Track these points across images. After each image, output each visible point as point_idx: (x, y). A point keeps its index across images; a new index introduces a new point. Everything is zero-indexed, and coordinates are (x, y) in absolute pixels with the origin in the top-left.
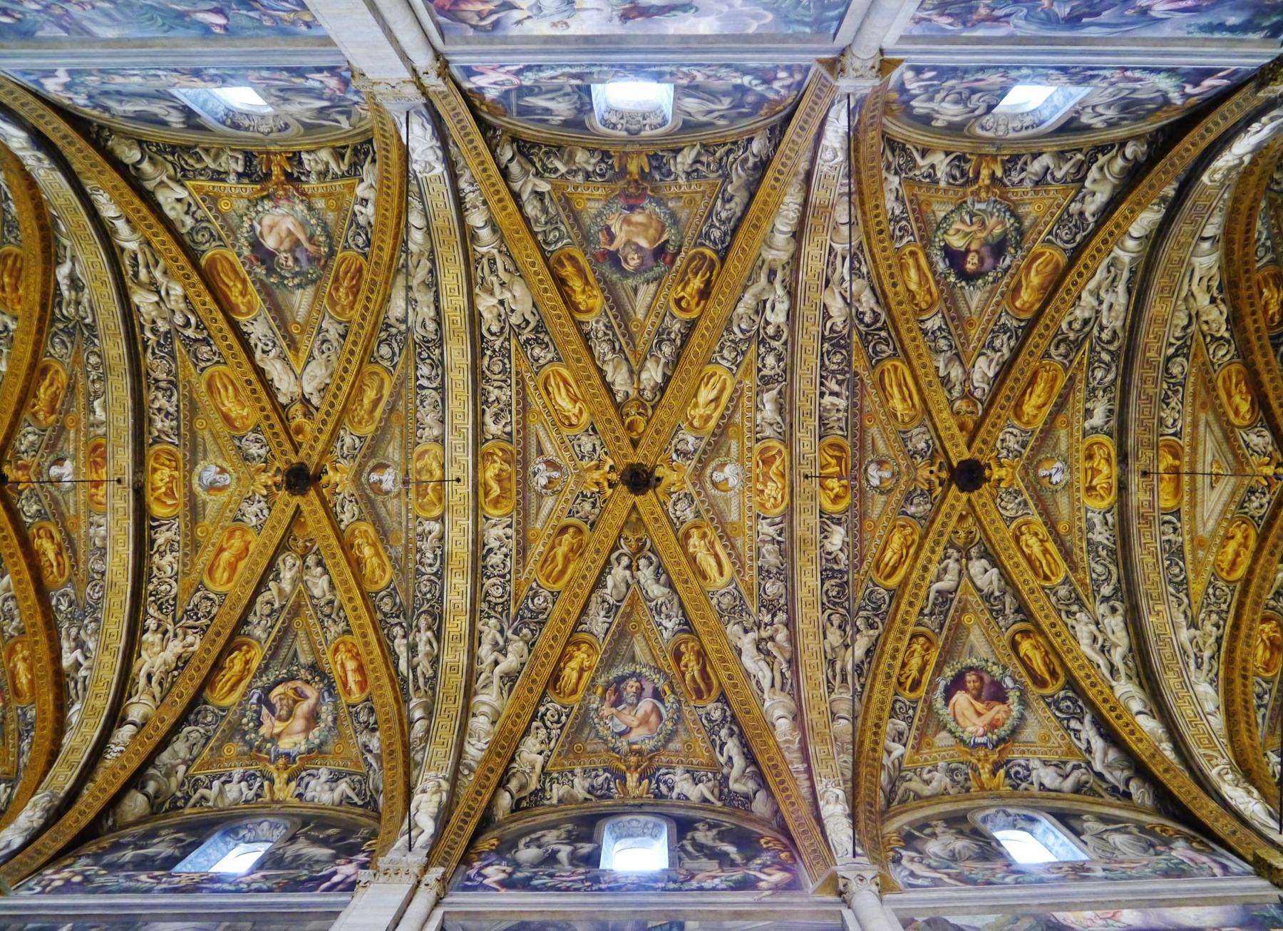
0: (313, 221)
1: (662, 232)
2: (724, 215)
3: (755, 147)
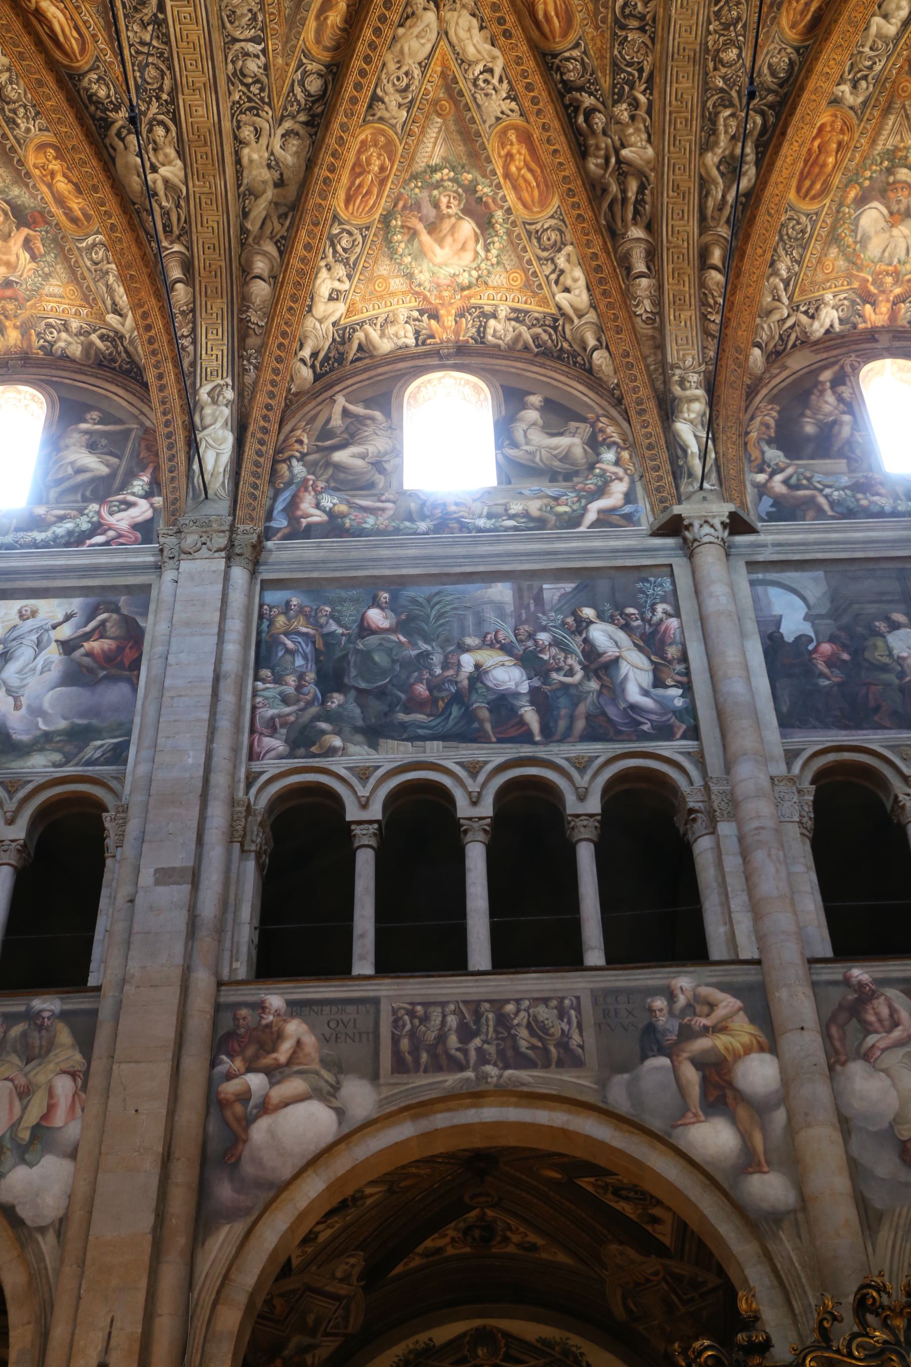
0: (408, 259)
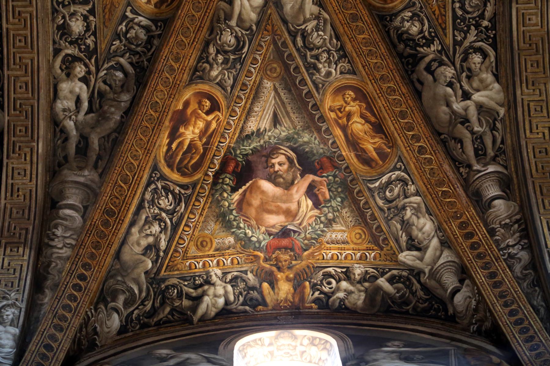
1: (241, 202)
2: (156, 228)
3: (115, 322)
